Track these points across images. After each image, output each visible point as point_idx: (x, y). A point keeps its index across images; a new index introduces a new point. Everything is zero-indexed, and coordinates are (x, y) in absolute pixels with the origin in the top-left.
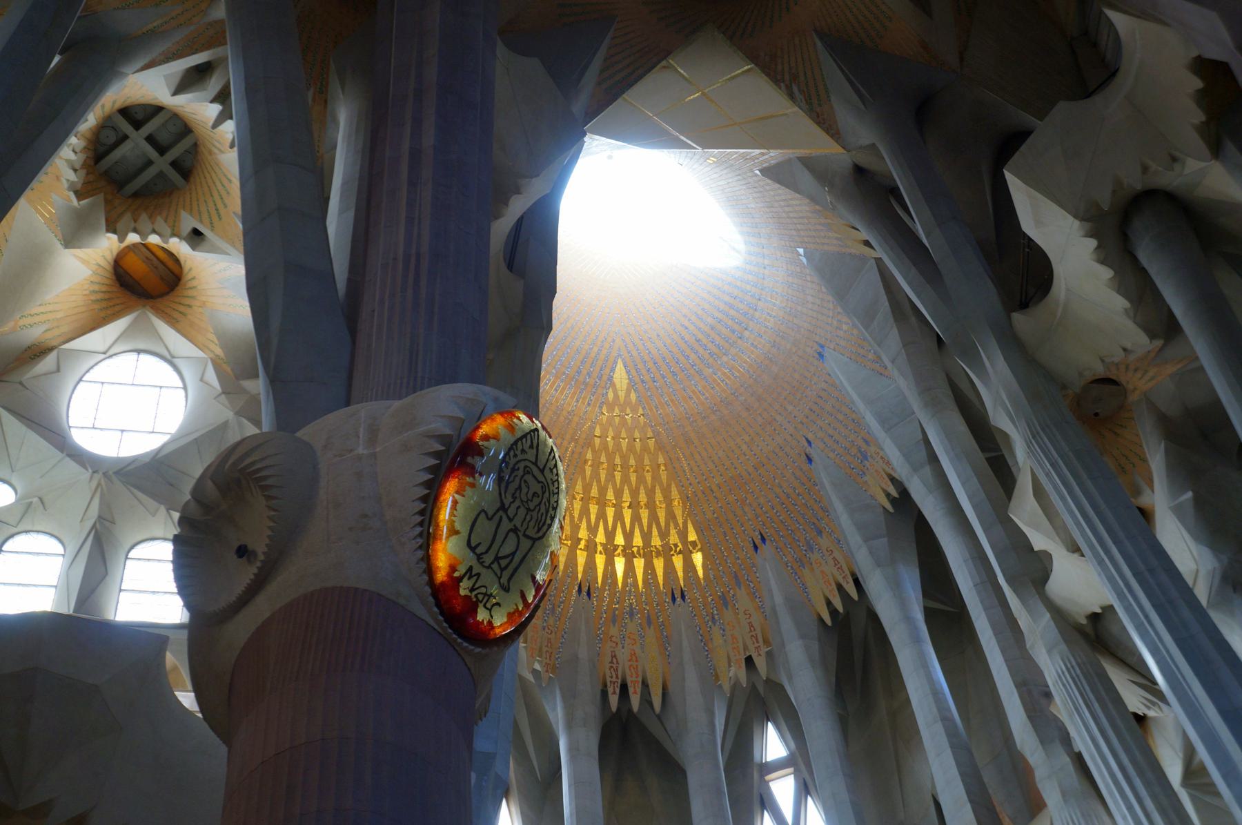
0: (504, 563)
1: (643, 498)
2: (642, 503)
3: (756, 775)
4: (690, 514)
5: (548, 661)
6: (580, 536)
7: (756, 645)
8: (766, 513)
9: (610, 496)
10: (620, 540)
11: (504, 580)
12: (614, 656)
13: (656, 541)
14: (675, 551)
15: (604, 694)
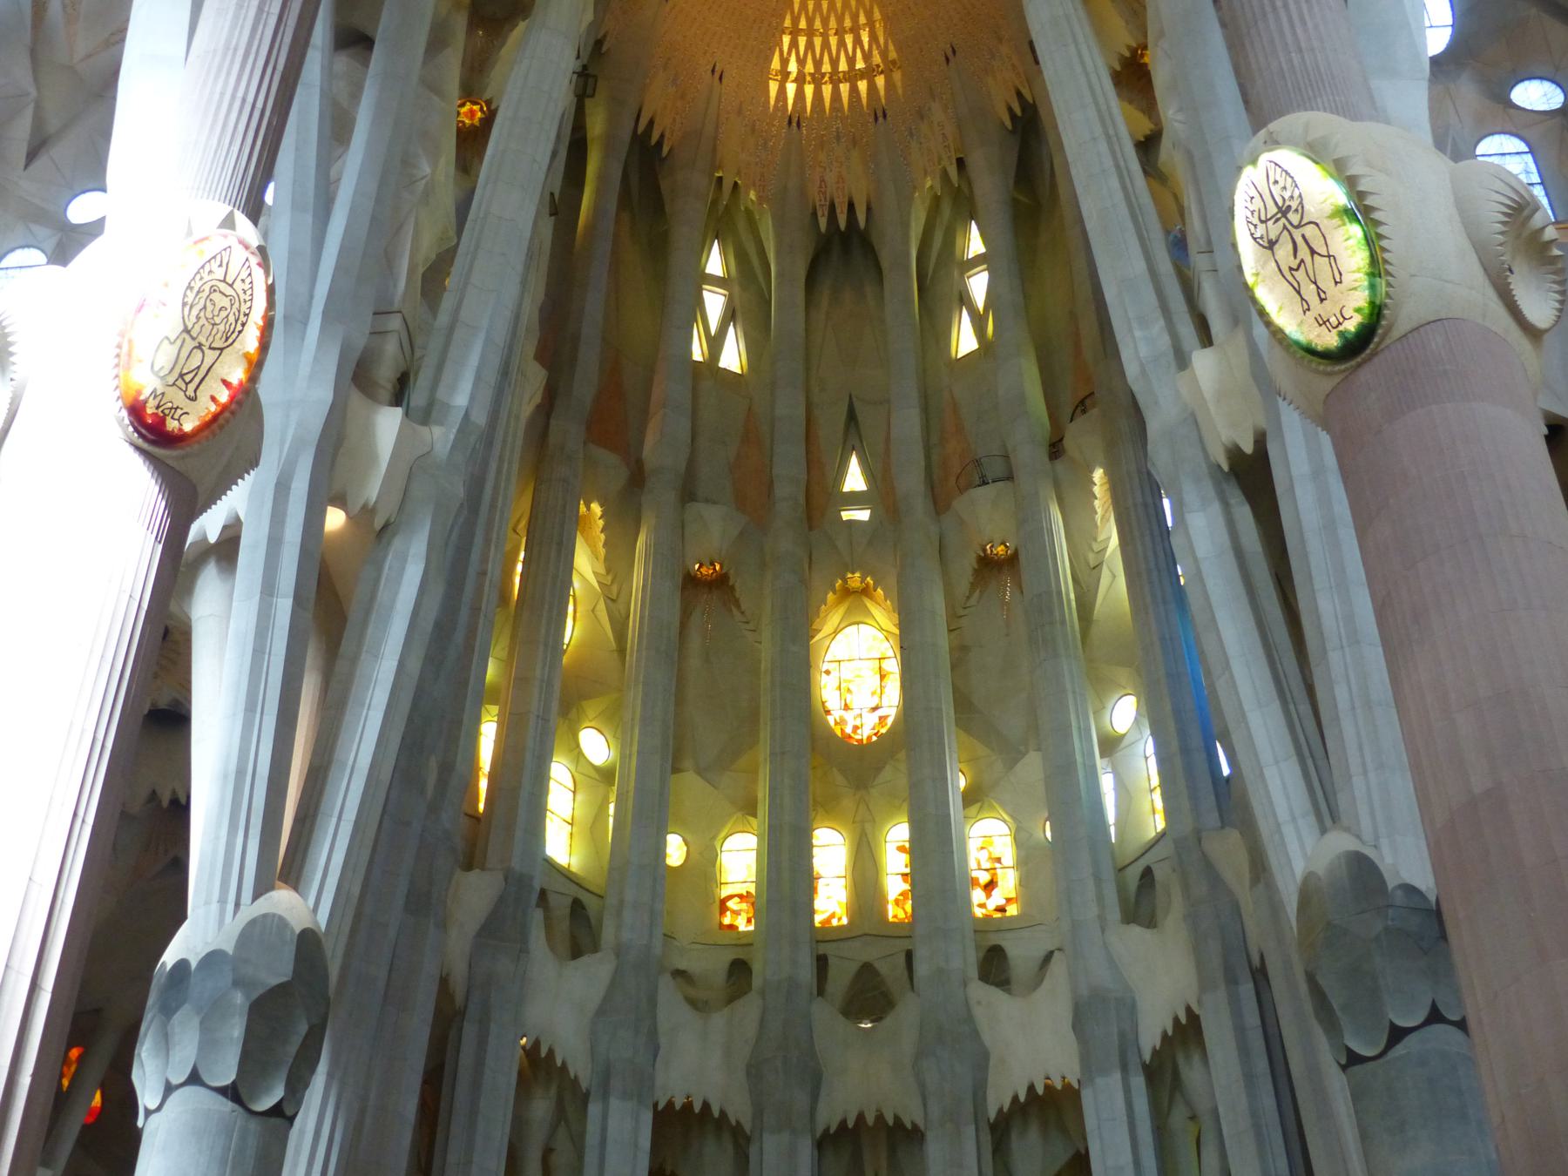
0: (188, 378)
1: (848, 23)
2: (847, 29)
3: (956, 273)
4: (889, 33)
5: (761, 194)
6: (789, 70)
7: (949, 154)
8: (955, 25)
9: (818, 24)
10: (826, 68)
11: (190, 392)
12: (823, 181)
13: (860, 65)
14: (878, 72)
15: (814, 214)
